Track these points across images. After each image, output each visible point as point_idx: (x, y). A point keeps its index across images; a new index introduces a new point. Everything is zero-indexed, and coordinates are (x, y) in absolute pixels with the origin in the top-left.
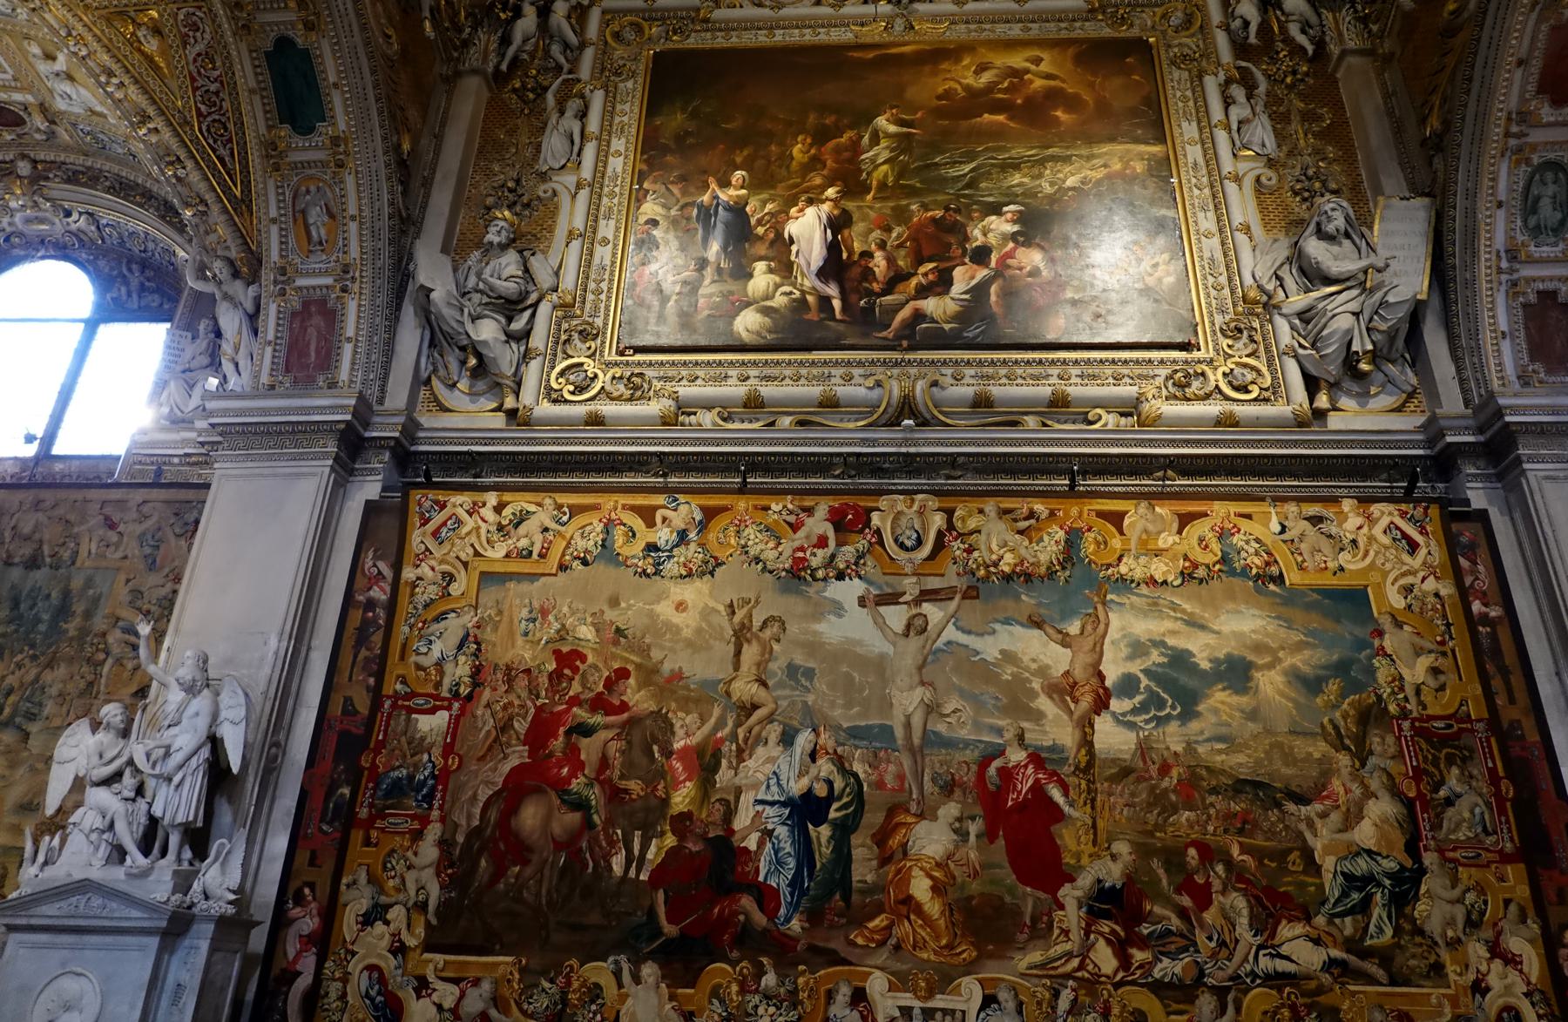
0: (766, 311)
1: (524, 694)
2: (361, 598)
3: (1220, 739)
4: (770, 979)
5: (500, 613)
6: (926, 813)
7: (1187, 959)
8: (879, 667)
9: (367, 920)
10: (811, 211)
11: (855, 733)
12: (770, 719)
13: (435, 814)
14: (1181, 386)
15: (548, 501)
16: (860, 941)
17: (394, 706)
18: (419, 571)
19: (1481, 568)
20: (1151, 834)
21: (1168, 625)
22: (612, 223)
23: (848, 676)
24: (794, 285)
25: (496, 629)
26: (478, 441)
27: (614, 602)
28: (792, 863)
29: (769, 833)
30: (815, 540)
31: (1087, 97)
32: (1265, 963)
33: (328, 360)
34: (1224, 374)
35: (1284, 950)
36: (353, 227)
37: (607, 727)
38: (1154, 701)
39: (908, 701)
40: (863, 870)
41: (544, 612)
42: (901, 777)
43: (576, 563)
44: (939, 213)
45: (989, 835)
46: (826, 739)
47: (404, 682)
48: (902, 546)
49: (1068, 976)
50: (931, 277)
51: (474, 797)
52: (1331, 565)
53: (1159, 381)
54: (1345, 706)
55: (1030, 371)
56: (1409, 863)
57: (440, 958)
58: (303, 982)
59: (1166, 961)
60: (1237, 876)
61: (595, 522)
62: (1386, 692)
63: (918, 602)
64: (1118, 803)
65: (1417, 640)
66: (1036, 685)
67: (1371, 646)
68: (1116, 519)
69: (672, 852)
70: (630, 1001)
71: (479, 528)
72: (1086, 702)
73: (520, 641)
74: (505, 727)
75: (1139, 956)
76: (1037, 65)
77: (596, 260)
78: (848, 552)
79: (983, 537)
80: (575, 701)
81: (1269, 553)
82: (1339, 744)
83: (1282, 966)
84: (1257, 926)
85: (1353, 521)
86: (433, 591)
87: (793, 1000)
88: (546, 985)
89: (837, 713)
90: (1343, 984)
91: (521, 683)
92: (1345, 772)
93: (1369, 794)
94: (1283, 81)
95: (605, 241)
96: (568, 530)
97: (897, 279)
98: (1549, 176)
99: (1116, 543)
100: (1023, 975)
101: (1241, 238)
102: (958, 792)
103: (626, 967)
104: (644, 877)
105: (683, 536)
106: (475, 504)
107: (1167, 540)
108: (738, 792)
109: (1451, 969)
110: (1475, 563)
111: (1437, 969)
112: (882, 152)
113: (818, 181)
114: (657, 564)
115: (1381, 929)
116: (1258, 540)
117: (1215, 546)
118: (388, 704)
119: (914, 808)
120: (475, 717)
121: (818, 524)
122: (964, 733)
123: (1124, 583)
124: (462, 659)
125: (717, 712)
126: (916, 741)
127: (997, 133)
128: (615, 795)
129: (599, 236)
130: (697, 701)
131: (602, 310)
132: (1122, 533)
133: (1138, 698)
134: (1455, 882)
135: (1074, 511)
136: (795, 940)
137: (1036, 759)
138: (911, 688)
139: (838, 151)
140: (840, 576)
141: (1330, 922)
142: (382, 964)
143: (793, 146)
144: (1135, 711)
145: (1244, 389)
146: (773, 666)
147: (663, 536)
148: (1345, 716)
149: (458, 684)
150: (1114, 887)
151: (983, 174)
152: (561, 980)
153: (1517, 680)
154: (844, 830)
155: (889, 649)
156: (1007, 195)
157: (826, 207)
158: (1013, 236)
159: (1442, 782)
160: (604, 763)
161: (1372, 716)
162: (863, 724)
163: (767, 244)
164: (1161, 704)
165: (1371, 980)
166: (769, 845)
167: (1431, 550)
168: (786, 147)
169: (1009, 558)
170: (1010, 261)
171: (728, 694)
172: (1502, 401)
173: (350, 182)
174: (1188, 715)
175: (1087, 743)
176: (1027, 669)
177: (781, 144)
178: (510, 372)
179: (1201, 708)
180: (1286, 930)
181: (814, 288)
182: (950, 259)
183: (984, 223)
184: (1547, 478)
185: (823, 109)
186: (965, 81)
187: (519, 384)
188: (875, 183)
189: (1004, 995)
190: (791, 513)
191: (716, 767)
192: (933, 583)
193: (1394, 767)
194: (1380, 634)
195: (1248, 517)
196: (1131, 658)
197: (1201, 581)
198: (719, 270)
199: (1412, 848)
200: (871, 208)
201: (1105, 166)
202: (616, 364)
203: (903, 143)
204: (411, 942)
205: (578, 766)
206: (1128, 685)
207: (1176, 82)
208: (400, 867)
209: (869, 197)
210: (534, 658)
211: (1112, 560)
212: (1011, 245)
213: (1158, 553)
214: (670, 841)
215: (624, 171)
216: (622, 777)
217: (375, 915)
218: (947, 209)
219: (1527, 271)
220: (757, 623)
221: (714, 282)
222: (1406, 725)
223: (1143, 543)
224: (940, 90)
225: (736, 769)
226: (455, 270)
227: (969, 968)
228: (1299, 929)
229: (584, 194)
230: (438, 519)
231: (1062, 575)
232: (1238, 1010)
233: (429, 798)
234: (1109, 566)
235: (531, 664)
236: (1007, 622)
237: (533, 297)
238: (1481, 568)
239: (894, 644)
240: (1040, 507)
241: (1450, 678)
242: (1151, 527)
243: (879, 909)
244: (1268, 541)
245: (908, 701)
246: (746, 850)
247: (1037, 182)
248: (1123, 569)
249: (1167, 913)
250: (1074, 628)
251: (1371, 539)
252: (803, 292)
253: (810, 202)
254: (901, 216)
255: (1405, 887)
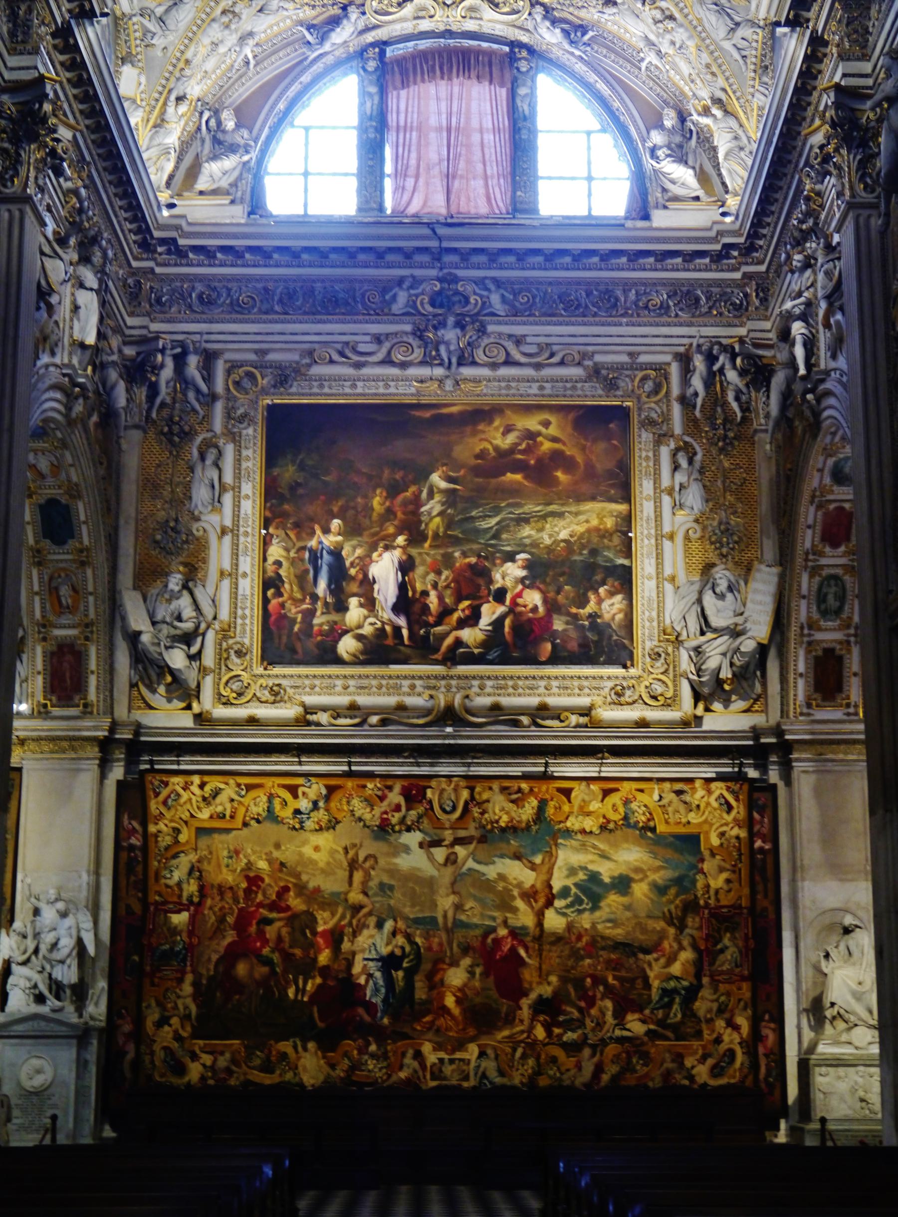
0: (360, 638)
1: (230, 901)
2: (125, 844)
3: (609, 921)
4: (373, 1048)
5: (211, 853)
6: (455, 963)
7: (580, 1032)
8: (430, 883)
9: (159, 1024)
10: (387, 555)
11: (417, 921)
12: (370, 914)
13: (189, 968)
14: (618, 694)
15: (231, 782)
16: (419, 1028)
17: (156, 909)
18: (158, 827)
19: (766, 820)
20: (568, 971)
21: (590, 857)
22: (248, 559)
23: (413, 889)
24: (376, 617)
25: (209, 863)
26: (179, 735)
27: (277, 846)
28: (383, 990)
29: (370, 976)
30: (393, 806)
31: (580, 459)
32: (618, 1033)
33: (80, 686)
34: (647, 687)
35: (628, 1026)
36: (91, 599)
37: (280, 919)
38: (578, 901)
39: (446, 902)
40: (420, 992)
41: (237, 852)
42: (441, 944)
43: (253, 822)
44: (473, 560)
45: (485, 974)
46: (401, 924)
47: (160, 895)
48: (444, 811)
49: (522, 1041)
50: (467, 612)
51: (209, 959)
52: (684, 820)
53: (607, 690)
54: (677, 902)
55: (527, 682)
56: (695, 982)
57: (201, 1042)
58: (131, 1056)
59: (570, 1034)
60: (610, 992)
61: (262, 795)
62: (699, 893)
63: (452, 845)
64: (554, 956)
65: (723, 864)
66: (516, 893)
67: (695, 867)
68: (567, 793)
69: (320, 987)
70: (303, 1060)
71: (190, 800)
72: (542, 901)
73: (224, 870)
74: (222, 920)
75: (557, 1031)
76: (547, 428)
77: (240, 592)
78: (413, 813)
79: (490, 805)
80: (260, 905)
81: (650, 814)
82: (670, 922)
83: (626, 1033)
84: (615, 1016)
85: (700, 793)
86: (168, 840)
87: (385, 1056)
88: (258, 1053)
89: (407, 911)
90: (653, 1041)
91: (229, 895)
92: (671, 937)
93: (681, 948)
94: (716, 444)
95: (245, 575)
96: (246, 801)
97: (445, 612)
98: (832, 582)
99: (566, 808)
100: (499, 1042)
101: (668, 587)
102: (471, 953)
103: (299, 1043)
104: (305, 999)
105: (315, 804)
106: (186, 783)
107: (594, 806)
108: (354, 954)
109: (706, 1033)
110: (763, 817)
111: (699, 1035)
112: (433, 506)
113: (391, 530)
114: (301, 822)
115: (676, 1014)
116: (645, 806)
117: (622, 810)
118: (152, 908)
119: (447, 960)
120: (204, 915)
121: (395, 797)
122: (475, 920)
123: (568, 833)
124: (192, 881)
125: (340, 910)
126: (450, 925)
127: (514, 491)
128: (287, 957)
129: (241, 571)
130: (329, 904)
131: (248, 631)
132: (570, 801)
133: (570, 899)
134: (716, 990)
135: (544, 788)
136: (384, 1028)
137: (516, 933)
138: (448, 895)
139: (405, 504)
140: (409, 829)
141: (652, 1012)
142: (171, 1046)
143: (373, 498)
144: (567, 907)
145: (655, 698)
146: (372, 884)
147: (304, 804)
148: (676, 907)
149: (191, 896)
150: (547, 999)
151: (503, 527)
152: (266, 1051)
153: (770, 885)
154: (410, 974)
155: (435, 873)
156: (519, 545)
157: (397, 553)
158: (522, 580)
159: (720, 940)
160: (280, 939)
161: (691, 907)
162: (420, 915)
163: (357, 583)
164: (581, 902)
165: (667, 1039)
166: (371, 982)
167: (739, 810)
168: (368, 498)
169: (505, 818)
170: (519, 601)
171: (346, 900)
172: (784, 727)
173: (89, 572)
174: (595, 907)
175: (540, 924)
176: (511, 884)
177: (365, 497)
178: (193, 685)
179: (602, 904)
180: (629, 1017)
181: (390, 620)
182: (480, 598)
183: (503, 569)
184: (804, 772)
185: (396, 464)
186: (495, 442)
187: (199, 692)
188: (430, 533)
189: (489, 1052)
190: (379, 789)
191: (341, 941)
192: (462, 833)
193: (695, 933)
194: (702, 860)
195: (642, 791)
196: (568, 876)
197: (611, 831)
198: (326, 604)
199: (698, 975)
200: (428, 554)
201: (587, 521)
202: (262, 676)
203: (451, 497)
204: (185, 1034)
205: (265, 942)
206: (565, 892)
207: (643, 440)
208: (173, 997)
209: (427, 545)
210: (234, 880)
211: (562, 819)
212: (520, 587)
213: (589, 814)
214: (318, 980)
215: (253, 514)
216: (291, 947)
217: (163, 1021)
218: (479, 556)
219: (819, 636)
220: (361, 858)
221: (323, 613)
222: (706, 911)
223: (581, 808)
224: (477, 450)
225: (352, 942)
226: (145, 600)
227: (472, 1039)
228: (636, 1016)
229: (227, 539)
230: (165, 793)
231: (534, 828)
232: (601, 1054)
233: (184, 960)
234: (561, 822)
235: (232, 884)
236: (502, 856)
237: (203, 626)
238: (766, 820)
239: (438, 870)
240: (524, 786)
241: (735, 885)
242: (587, 798)
243: (427, 1012)
244: (651, 806)
245: (446, 902)
246: (359, 984)
247: (540, 535)
248: (568, 824)
249: (573, 1010)
250: (538, 859)
251: (708, 804)
252: (383, 623)
253: (387, 548)
254: (448, 561)
255: (692, 993)
